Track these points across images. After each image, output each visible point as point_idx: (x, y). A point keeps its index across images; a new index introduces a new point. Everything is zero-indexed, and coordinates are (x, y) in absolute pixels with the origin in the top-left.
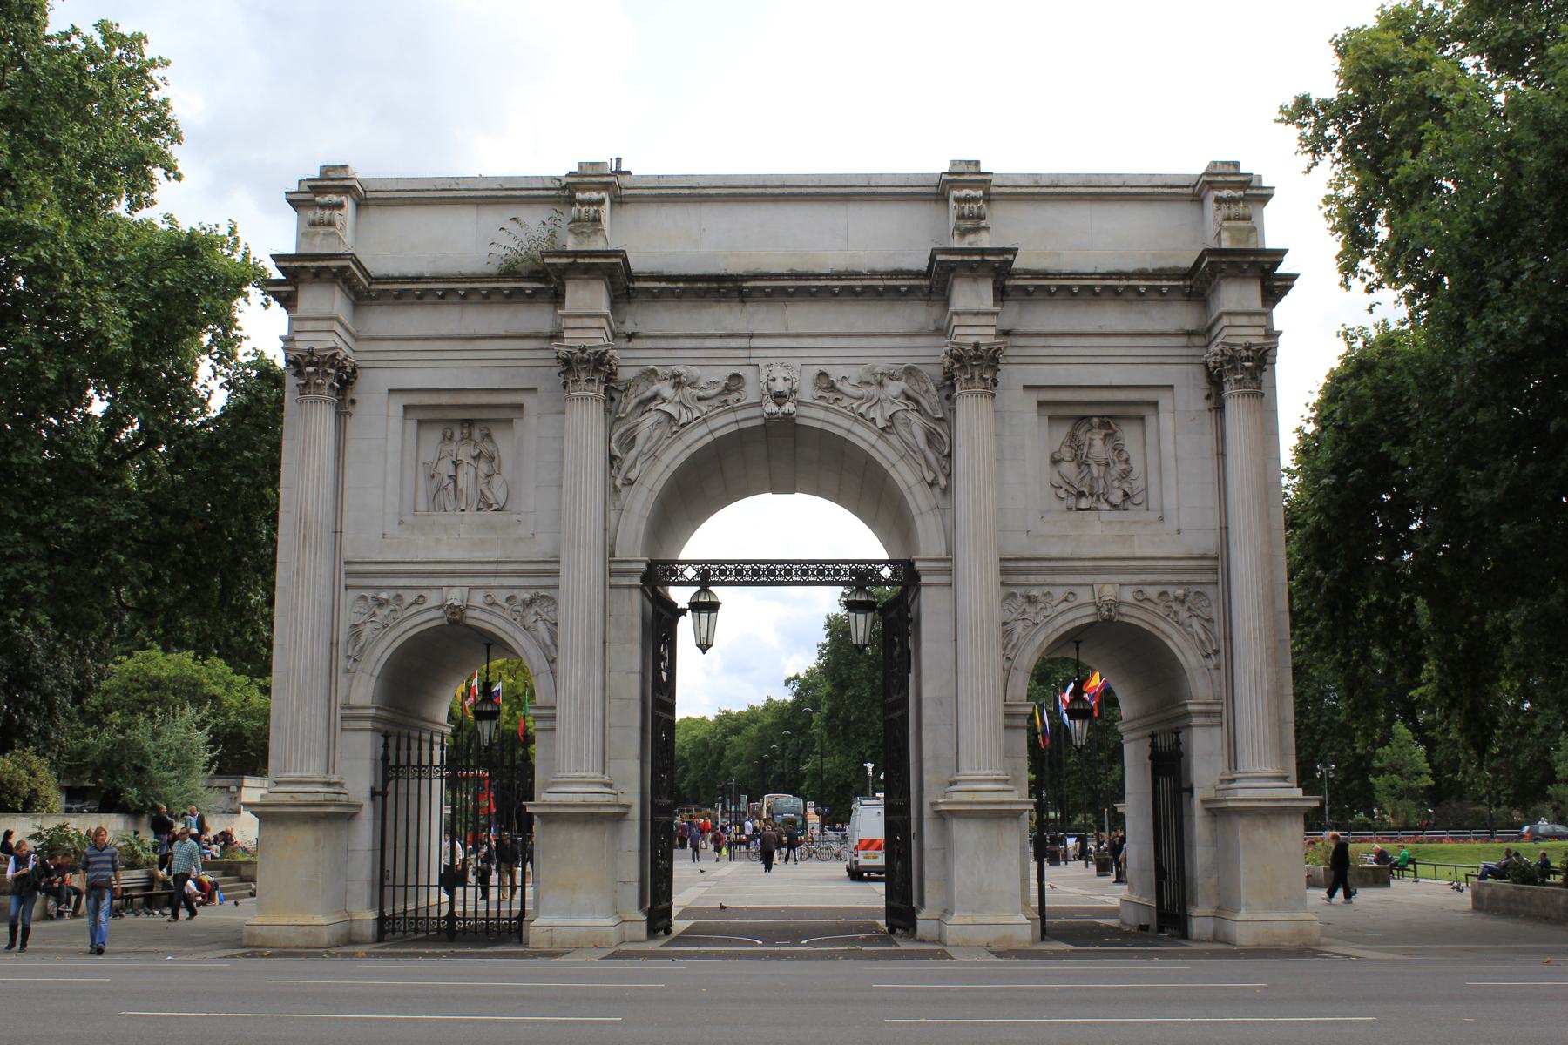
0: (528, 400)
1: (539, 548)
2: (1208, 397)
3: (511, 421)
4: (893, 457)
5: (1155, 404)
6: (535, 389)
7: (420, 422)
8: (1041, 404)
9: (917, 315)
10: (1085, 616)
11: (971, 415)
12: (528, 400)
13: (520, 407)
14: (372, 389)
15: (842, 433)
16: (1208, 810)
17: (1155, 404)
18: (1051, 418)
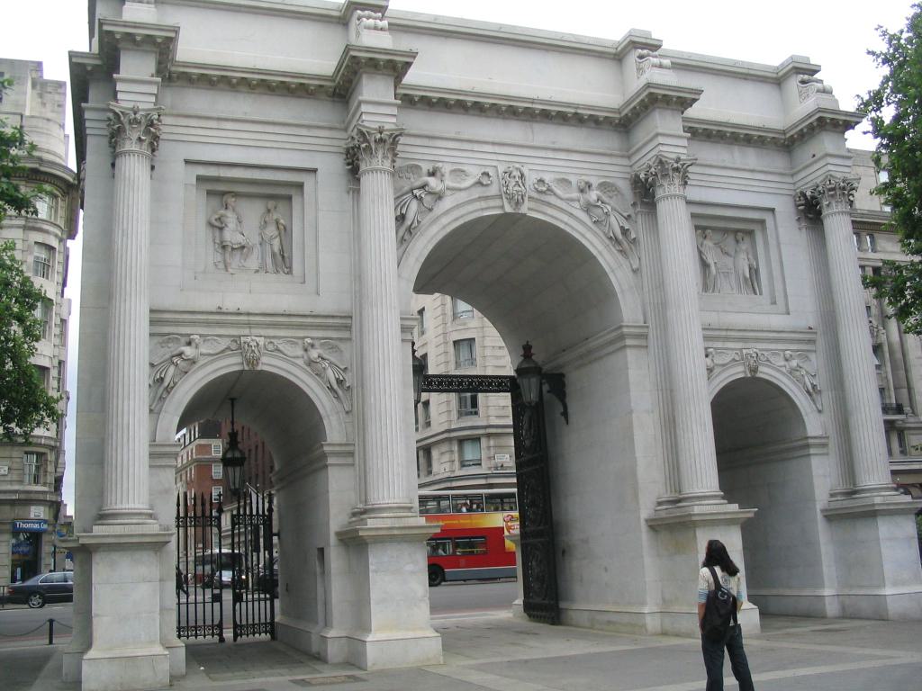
0: (308, 181)
1: (329, 301)
2: (799, 220)
3: (289, 198)
4: (601, 247)
5: (762, 222)
6: (315, 171)
7: (210, 193)
8: (694, 216)
12: (308, 181)
13: (300, 186)
14: (173, 154)
15: (562, 226)
16: (825, 516)
17: (762, 222)
18: (697, 228)
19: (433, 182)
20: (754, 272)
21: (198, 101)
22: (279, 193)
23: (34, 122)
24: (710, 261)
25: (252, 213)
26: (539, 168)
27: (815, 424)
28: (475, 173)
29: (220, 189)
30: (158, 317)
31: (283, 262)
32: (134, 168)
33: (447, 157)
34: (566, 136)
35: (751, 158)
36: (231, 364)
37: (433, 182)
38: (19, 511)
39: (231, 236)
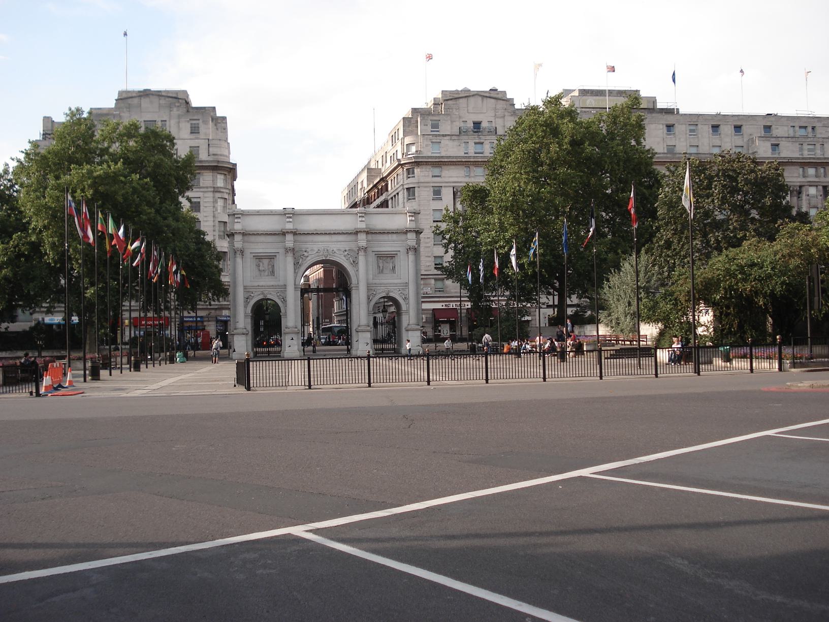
1: (281, 283)
9: (352, 237)
10: (384, 295)
11: (361, 259)
19: (306, 254)
20: (394, 268)
21: (253, 238)
22: (272, 257)
23: (214, 142)
24: (381, 265)
25: (266, 262)
26: (334, 247)
27: (404, 307)
28: (316, 250)
29: (259, 258)
30: (245, 288)
31: (273, 273)
32: (239, 260)
33: (309, 246)
34: (341, 238)
35: (394, 237)
36: (261, 297)
37: (306, 254)
38: (218, 312)
39: (261, 268)
